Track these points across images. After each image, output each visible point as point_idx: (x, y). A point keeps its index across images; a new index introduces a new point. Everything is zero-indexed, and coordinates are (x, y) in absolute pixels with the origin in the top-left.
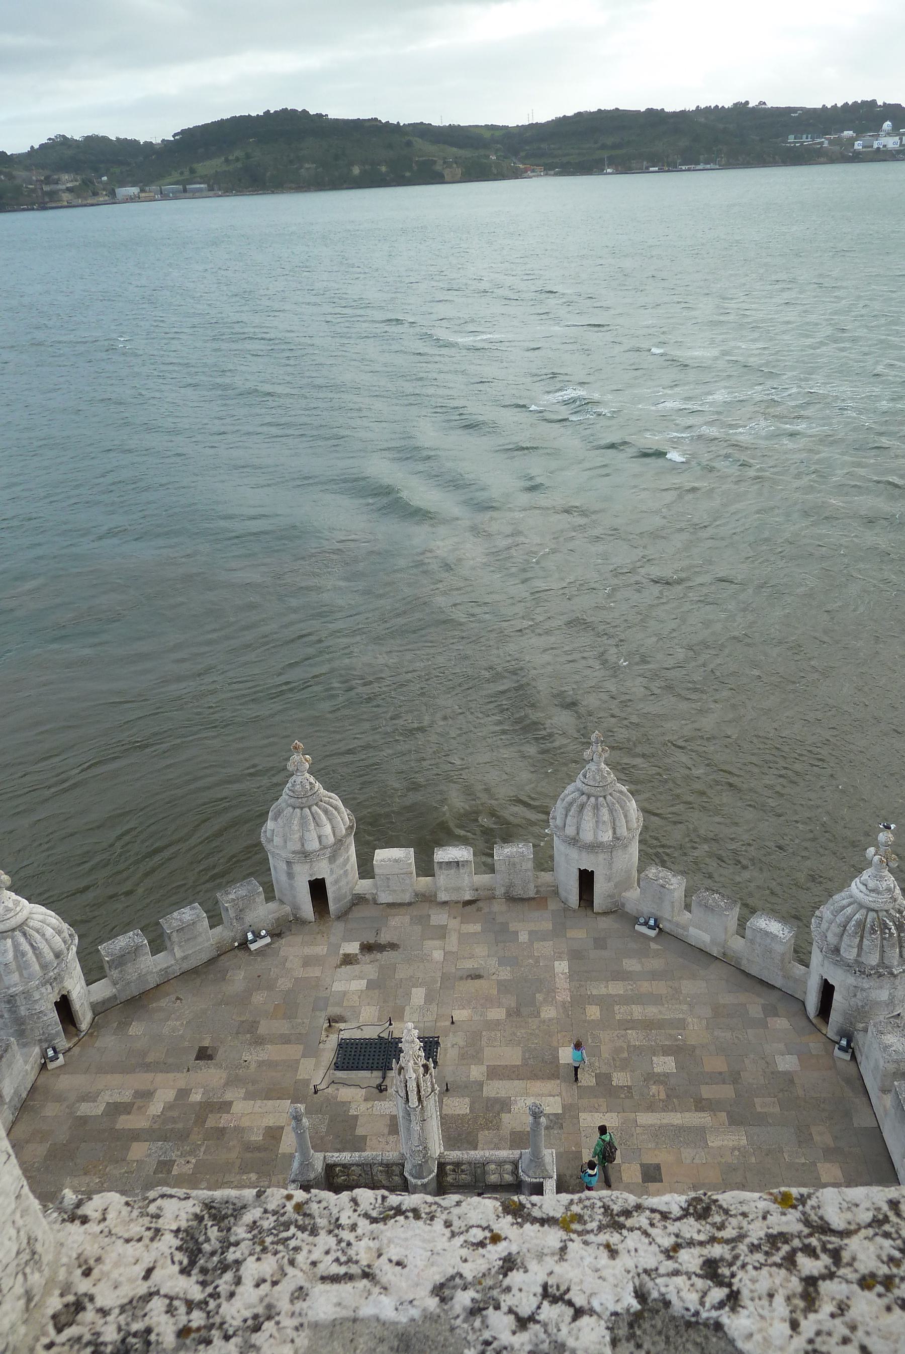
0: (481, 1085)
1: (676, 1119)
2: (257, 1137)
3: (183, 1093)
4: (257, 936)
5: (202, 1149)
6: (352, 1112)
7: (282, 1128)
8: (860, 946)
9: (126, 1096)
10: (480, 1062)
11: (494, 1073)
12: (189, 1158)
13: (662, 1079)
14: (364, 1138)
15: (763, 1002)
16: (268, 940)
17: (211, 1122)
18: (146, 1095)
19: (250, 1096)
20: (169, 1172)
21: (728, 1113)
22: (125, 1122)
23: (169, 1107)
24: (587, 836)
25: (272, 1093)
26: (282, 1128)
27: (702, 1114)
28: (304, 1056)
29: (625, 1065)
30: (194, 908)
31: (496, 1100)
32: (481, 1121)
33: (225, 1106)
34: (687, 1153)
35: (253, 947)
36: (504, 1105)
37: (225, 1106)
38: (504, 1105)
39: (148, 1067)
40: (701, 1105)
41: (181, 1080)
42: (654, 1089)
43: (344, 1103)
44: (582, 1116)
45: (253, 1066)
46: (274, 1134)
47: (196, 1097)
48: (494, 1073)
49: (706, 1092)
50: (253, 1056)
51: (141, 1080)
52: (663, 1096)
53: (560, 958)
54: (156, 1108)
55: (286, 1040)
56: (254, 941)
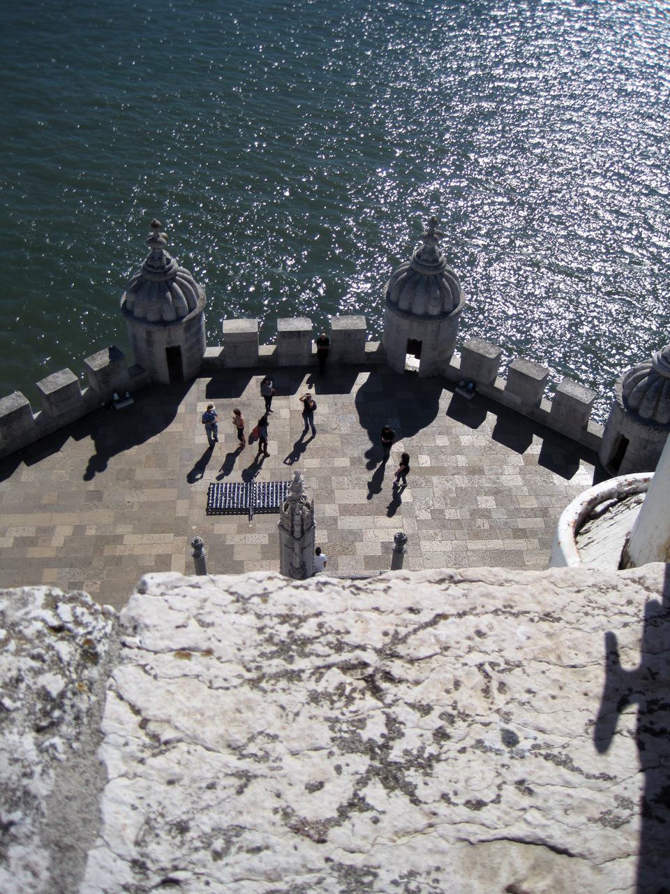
0: (335, 520)
3: (79, 530)
4: (123, 398)
5: (105, 573)
6: (228, 542)
7: (170, 556)
8: (656, 408)
9: (31, 532)
10: (332, 501)
11: (347, 510)
14: (242, 562)
16: (132, 401)
18: (48, 531)
19: (139, 531)
21: (540, 539)
22: (33, 553)
23: (68, 540)
24: (418, 310)
26: (170, 556)
27: (519, 541)
28: (179, 498)
29: (454, 503)
30: (66, 373)
31: (351, 532)
32: (338, 548)
33: (118, 539)
35: (119, 407)
36: (357, 535)
37: (118, 539)
38: (357, 535)
39: (43, 508)
40: (519, 533)
41: (75, 518)
42: (479, 522)
43: (219, 536)
44: (423, 543)
45: (136, 508)
47: (91, 532)
48: (347, 510)
49: (521, 523)
50: (132, 498)
51: (40, 519)
54: (58, 540)
55: (162, 485)
56: (118, 402)
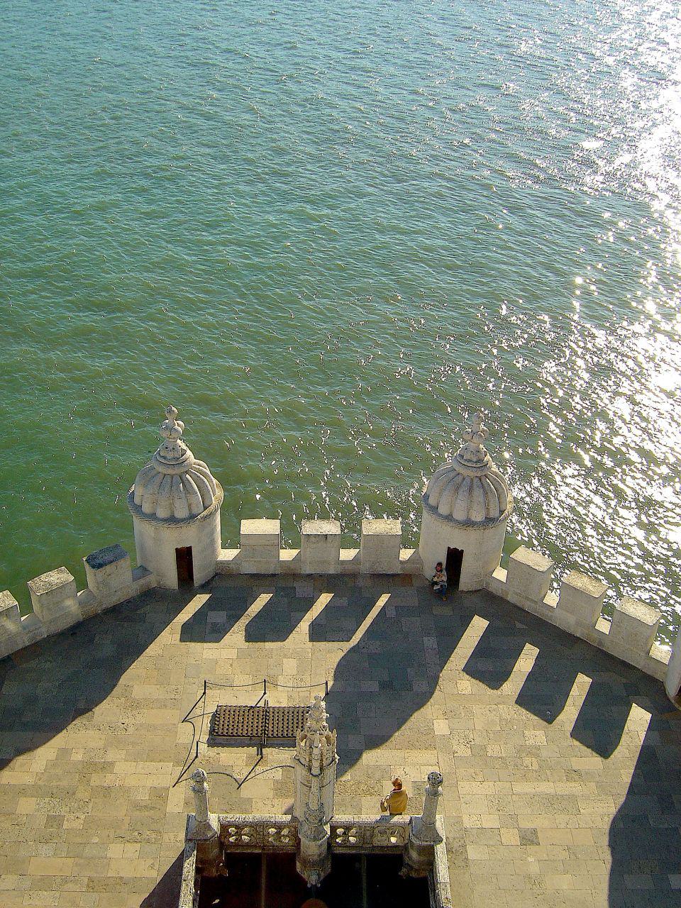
1: (546, 788)
2: (143, 797)
12: (78, 814)
13: (534, 751)
14: (250, 800)
15: (624, 680)
17: (96, 780)
20: (60, 825)
25: (153, 755)
27: (573, 784)
30: (62, 571)
33: (107, 767)
34: (561, 819)
37: (107, 767)
42: (527, 761)
46: (160, 795)
47: (78, 757)
52: (536, 767)
53: (429, 634)
